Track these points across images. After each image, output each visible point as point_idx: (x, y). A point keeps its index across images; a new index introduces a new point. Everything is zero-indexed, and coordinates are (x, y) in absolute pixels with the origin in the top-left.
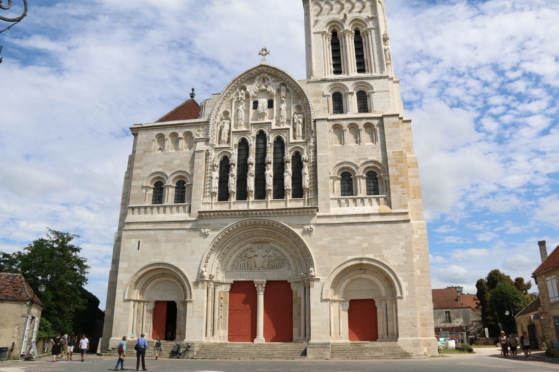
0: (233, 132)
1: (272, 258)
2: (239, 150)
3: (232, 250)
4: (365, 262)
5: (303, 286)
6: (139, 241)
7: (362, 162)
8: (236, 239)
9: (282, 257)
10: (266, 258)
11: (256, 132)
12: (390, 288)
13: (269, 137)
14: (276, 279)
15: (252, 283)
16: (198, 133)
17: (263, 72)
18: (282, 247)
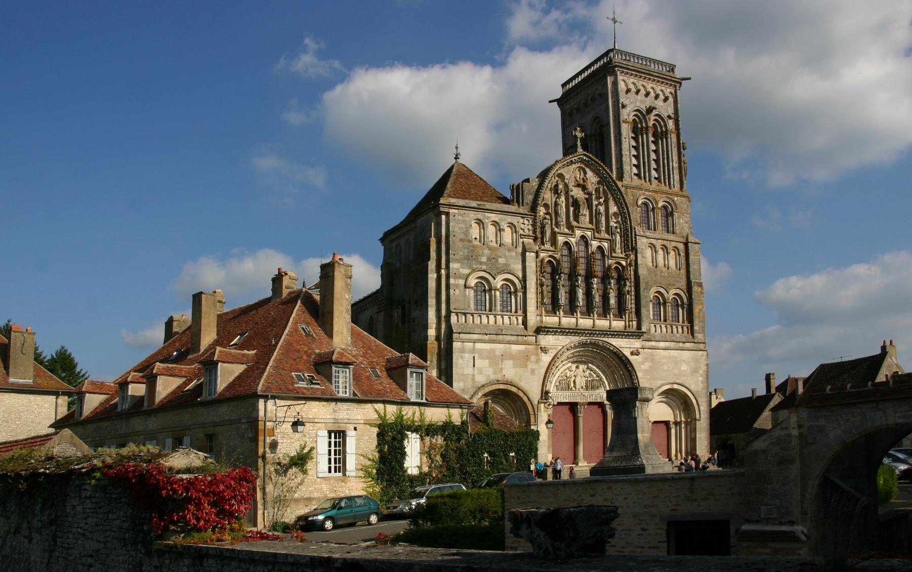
4: (676, 386)
6: (474, 357)
12: (686, 412)
13: (591, 246)
16: (522, 226)
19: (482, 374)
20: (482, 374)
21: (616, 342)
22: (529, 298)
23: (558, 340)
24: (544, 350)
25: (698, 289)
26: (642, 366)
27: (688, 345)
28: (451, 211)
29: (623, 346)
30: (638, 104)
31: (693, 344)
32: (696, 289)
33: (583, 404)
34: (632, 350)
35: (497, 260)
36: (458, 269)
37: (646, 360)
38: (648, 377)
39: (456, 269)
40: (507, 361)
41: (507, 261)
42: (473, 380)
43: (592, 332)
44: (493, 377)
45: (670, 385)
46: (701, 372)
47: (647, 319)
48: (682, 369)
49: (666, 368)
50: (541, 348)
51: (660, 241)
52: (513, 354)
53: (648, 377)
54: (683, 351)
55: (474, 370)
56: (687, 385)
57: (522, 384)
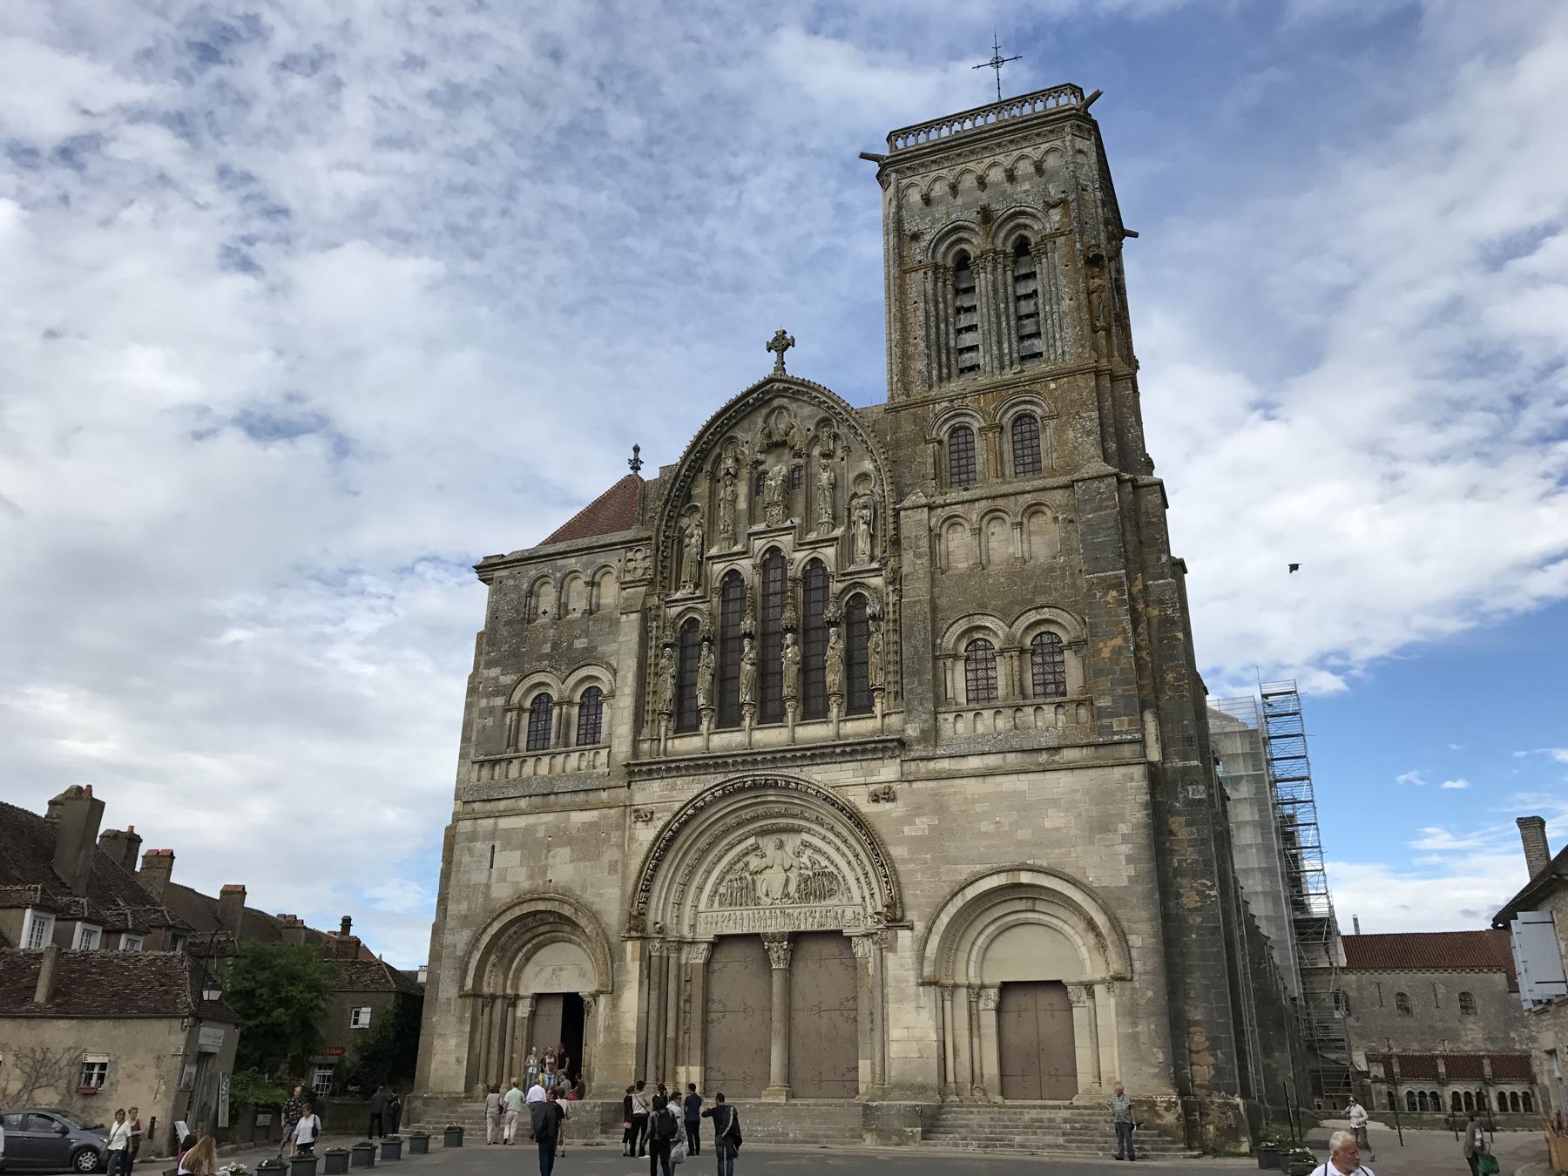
0: (709, 558)
1: (807, 872)
2: (724, 602)
3: (711, 857)
4: (1025, 878)
5: (877, 946)
6: (493, 847)
7: (1017, 609)
8: (716, 827)
9: (832, 869)
10: (793, 875)
11: (762, 553)
14: (815, 928)
15: (754, 938)
17: (780, 394)
18: (829, 843)
19: (505, 881)
20: (505, 881)
21: (821, 775)
22: (620, 708)
23: (673, 788)
24: (648, 818)
25: (1106, 594)
26: (906, 829)
27: (1069, 755)
28: (496, 574)
29: (842, 782)
30: (954, 217)
31: (1093, 748)
32: (1098, 595)
33: (774, 938)
34: (872, 788)
35: (572, 644)
36: (496, 679)
37: (917, 810)
38: (929, 856)
39: (493, 678)
40: (558, 849)
41: (590, 641)
42: (487, 896)
43: (750, 757)
44: (526, 885)
45: (1003, 875)
46: (1124, 828)
47: (921, 704)
48: (1047, 824)
49: (986, 826)
50: (636, 811)
51: (984, 503)
52: (574, 832)
53: (929, 856)
54: (1049, 775)
55: (490, 874)
56: (1069, 870)
57: (588, 897)
